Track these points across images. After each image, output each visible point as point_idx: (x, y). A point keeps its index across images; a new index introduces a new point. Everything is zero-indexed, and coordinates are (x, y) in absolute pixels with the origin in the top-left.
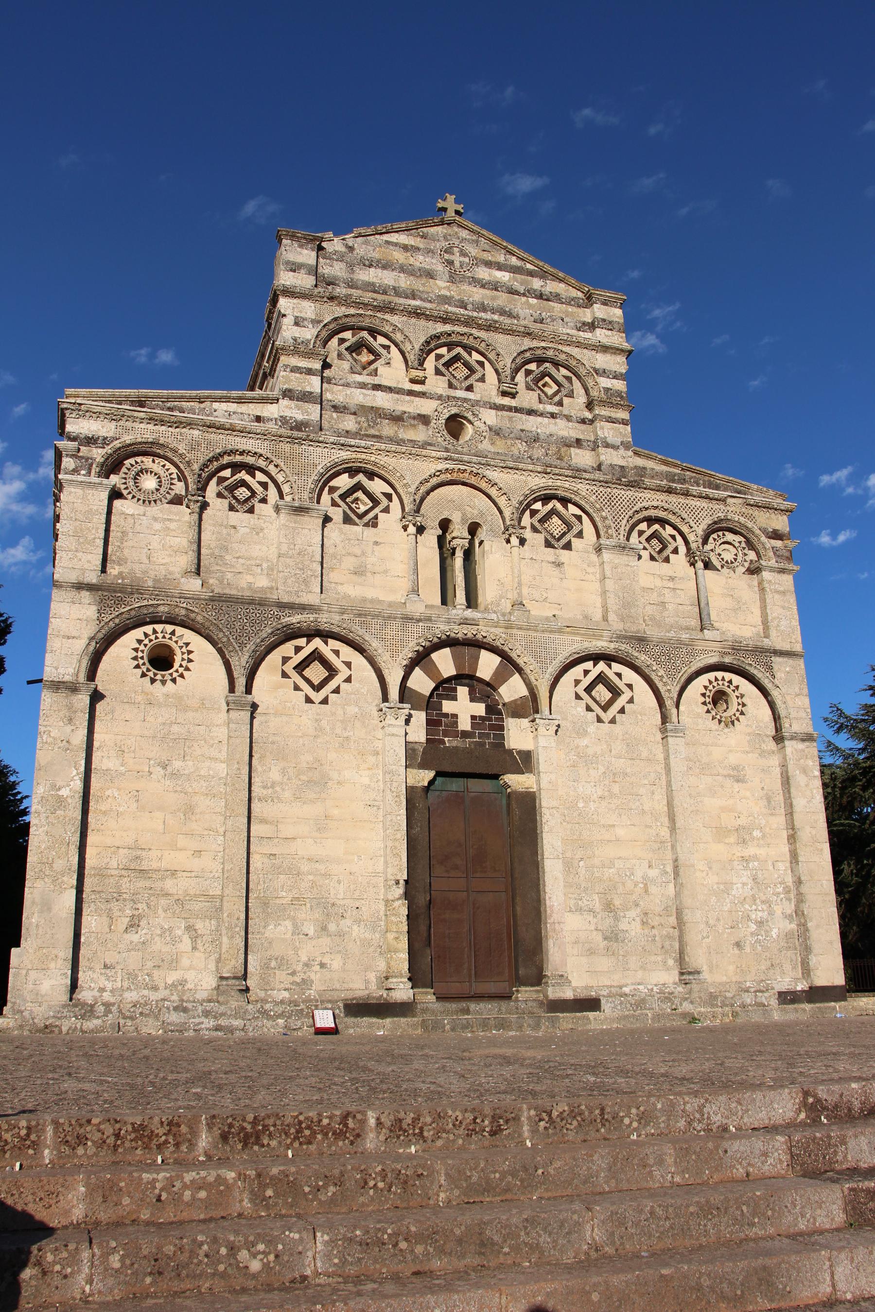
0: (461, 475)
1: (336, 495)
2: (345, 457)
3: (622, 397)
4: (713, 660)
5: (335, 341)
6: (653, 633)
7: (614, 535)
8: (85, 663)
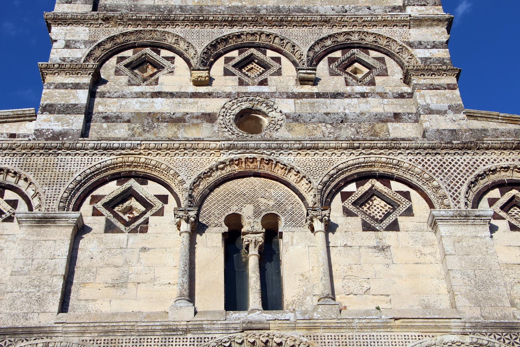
0: (251, 166)
1: (99, 205)
2: (109, 162)
3: (444, 64)
5: (113, 60)
7: (452, 205)
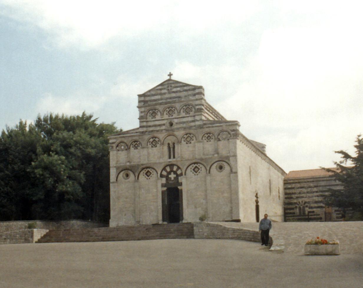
4: (217, 160)
6: (203, 157)
8: (116, 179)
